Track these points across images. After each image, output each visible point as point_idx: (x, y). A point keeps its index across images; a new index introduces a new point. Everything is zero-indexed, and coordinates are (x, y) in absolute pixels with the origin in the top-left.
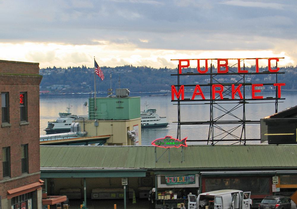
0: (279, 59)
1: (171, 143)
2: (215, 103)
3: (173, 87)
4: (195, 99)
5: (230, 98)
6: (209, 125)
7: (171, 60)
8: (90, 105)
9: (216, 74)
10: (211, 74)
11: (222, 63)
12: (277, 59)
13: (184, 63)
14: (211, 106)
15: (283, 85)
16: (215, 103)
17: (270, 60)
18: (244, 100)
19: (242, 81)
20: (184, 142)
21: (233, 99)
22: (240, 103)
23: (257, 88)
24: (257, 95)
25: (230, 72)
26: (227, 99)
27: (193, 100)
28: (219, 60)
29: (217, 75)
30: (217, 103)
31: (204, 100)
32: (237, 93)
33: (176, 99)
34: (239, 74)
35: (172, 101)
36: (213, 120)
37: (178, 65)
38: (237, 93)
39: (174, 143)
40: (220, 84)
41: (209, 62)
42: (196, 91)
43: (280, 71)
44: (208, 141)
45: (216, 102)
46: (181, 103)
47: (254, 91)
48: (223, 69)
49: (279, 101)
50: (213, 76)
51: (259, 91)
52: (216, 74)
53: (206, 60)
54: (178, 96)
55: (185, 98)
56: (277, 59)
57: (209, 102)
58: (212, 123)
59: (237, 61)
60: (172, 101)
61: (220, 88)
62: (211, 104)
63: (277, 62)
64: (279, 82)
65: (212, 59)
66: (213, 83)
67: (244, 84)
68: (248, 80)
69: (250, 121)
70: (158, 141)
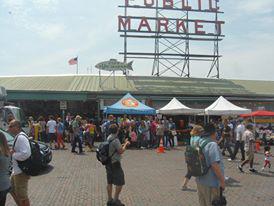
3: (120, 18)
5: (175, 30)
10: (157, 8)
15: (223, 23)
21: (177, 33)
23: (199, 24)
24: (199, 29)
27: (139, 31)
31: (150, 31)
32: (181, 27)
33: (122, 28)
38: (181, 27)
46: (128, 34)
47: (197, 26)
51: (202, 27)
54: (124, 26)
58: (157, 55)
61: (165, 22)
64: (219, 20)
67: (187, 20)
68: (192, 16)
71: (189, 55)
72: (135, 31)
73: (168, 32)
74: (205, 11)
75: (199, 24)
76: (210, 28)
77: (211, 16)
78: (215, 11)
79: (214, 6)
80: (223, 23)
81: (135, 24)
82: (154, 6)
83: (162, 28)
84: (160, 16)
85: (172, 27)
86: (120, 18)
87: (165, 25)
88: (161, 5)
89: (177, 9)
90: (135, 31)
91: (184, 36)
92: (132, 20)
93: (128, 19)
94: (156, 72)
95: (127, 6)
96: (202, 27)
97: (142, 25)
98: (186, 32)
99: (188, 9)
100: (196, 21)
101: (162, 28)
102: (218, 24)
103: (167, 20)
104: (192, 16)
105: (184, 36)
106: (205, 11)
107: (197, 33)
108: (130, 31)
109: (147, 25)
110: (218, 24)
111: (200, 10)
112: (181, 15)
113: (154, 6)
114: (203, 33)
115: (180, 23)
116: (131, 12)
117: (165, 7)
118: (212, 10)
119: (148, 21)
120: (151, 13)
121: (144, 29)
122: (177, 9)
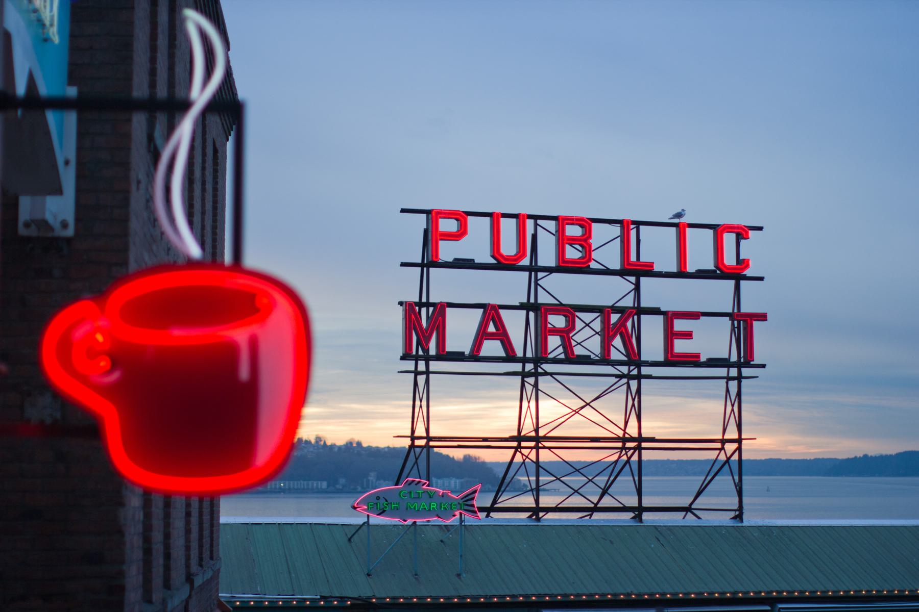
0: (751, 233)
1: (424, 505)
2: (546, 373)
4: (483, 353)
6: (513, 450)
7: (403, 211)
8: (681, 229)
9: (550, 270)
10: (533, 269)
11: (573, 231)
12: (741, 233)
13: (448, 225)
14: (529, 388)
15: (763, 317)
16: (546, 373)
17: (718, 230)
18: (639, 364)
19: (629, 302)
20: (469, 503)
21: (605, 360)
22: (620, 377)
23: (680, 325)
24: (681, 346)
25: (593, 265)
26: (585, 360)
27: (475, 357)
28: (561, 222)
29: (554, 274)
30: (551, 374)
31: (510, 357)
32: (618, 342)
34: (621, 273)
35: (402, 358)
36: (537, 430)
37: (426, 232)
38: (618, 342)
39: (434, 505)
40: (561, 304)
41: (530, 223)
42: (483, 326)
43: (748, 273)
44: (489, 510)
45: (548, 367)
46: (434, 366)
47: (670, 335)
48: (572, 253)
49: (746, 372)
50: (540, 275)
51: (688, 335)
52: (550, 270)
53: (520, 219)
55: (450, 347)
56: (741, 233)
57: (518, 367)
59: (616, 230)
60: (402, 358)
62: (524, 375)
63: (743, 242)
65: (536, 218)
66: (541, 300)
67: (640, 311)
68: (654, 292)
69: (652, 440)
70: (378, 498)
71: (640, 439)
72: (458, 357)
73: (571, 358)
74: (701, 274)
75: (680, 325)
76: (712, 339)
77: (719, 294)
78: (736, 274)
79: (730, 260)
80: (763, 317)
81: (461, 329)
82: (526, 262)
83: (554, 342)
84: (544, 298)
85: (588, 340)
86: (411, 311)
87: (565, 334)
88: (547, 256)
89: (607, 272)
90: (458, 357)
91: (624, 369)
92: (449, 311)
93: (440, 309)
94: (420, 431)
95: (430, 262)
96: (688, 335)
97: (482, 335)
98: (634, 358)
99: (647, 270)
100: (670, 317)
101: (554, 342)
102: (744, 323)
103: (570, 311)
104: (654, 292)
105: (624, 369)
106: (701, 274)
107: (672, 359)
108: (444, 355)
109: (502, 335)
110: (744, 323)
111: (682, 274)
112: (614, 291)
113: (526, 262)
114: (692, 360)
115: (619, 322)
116: (445, 286)
117: (564, 267)
118: (720, 273)
119: (501, 312)
120: (510, 287)
121: (492, 348)
122: (607, 272)
